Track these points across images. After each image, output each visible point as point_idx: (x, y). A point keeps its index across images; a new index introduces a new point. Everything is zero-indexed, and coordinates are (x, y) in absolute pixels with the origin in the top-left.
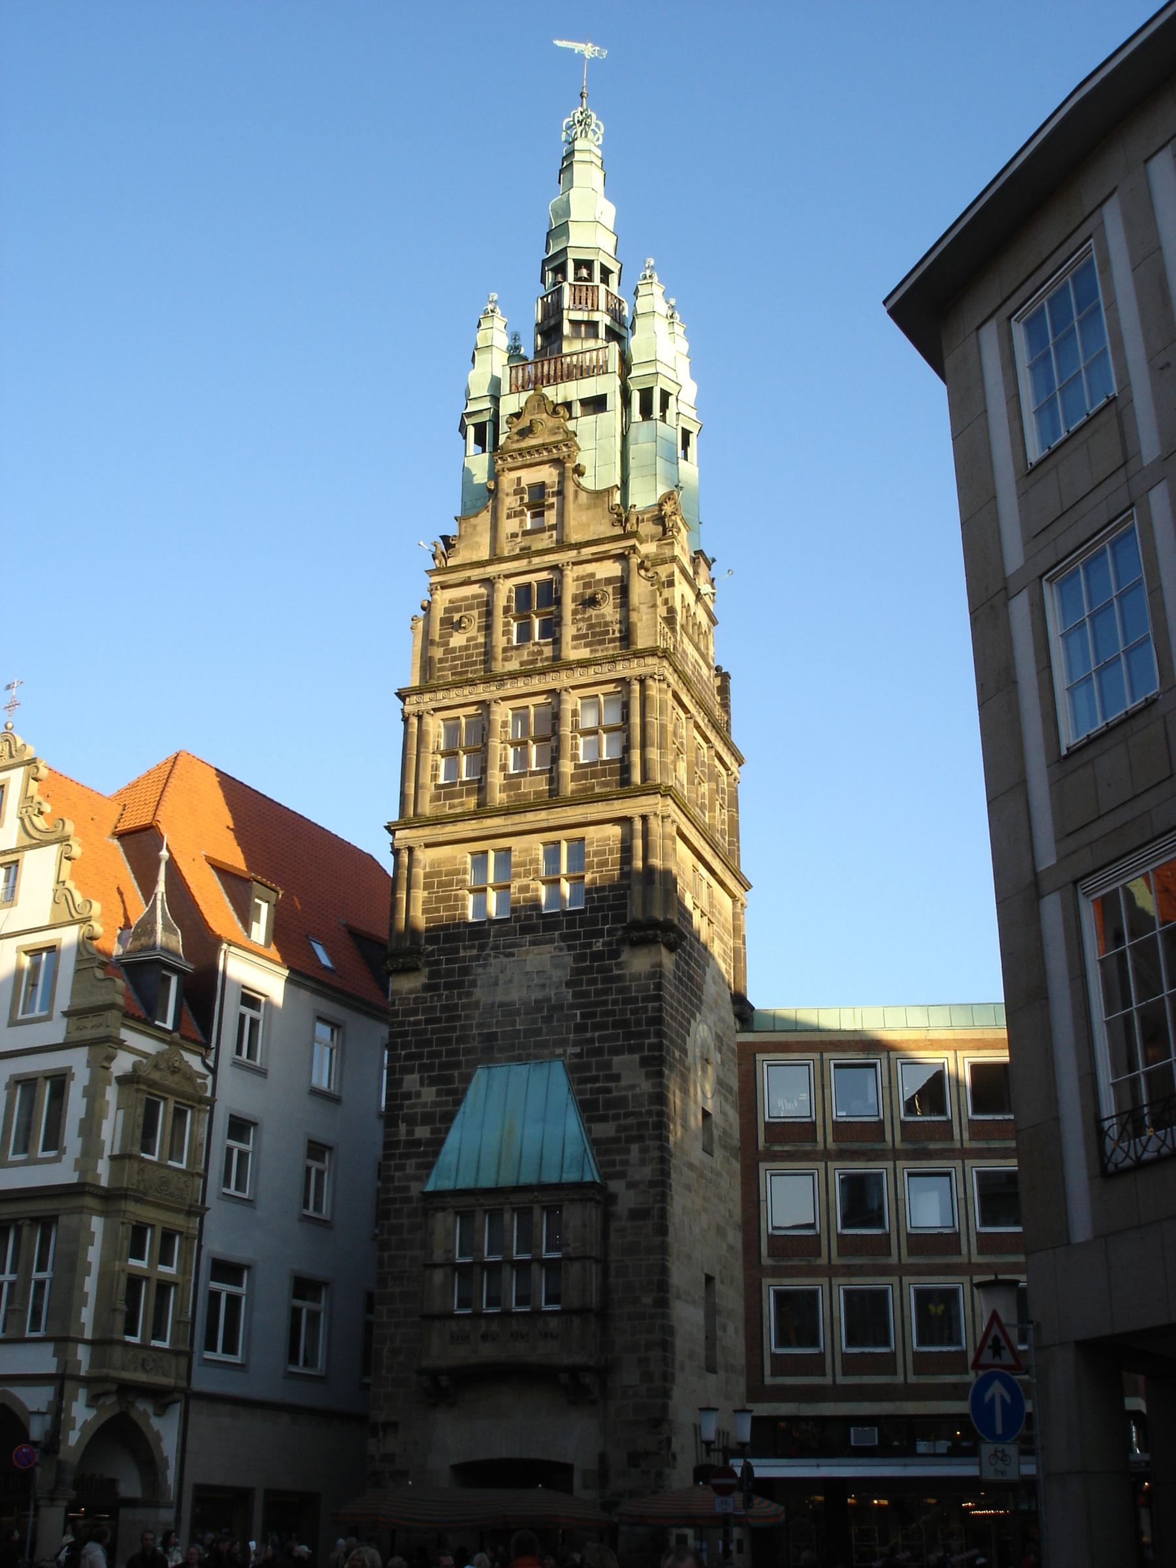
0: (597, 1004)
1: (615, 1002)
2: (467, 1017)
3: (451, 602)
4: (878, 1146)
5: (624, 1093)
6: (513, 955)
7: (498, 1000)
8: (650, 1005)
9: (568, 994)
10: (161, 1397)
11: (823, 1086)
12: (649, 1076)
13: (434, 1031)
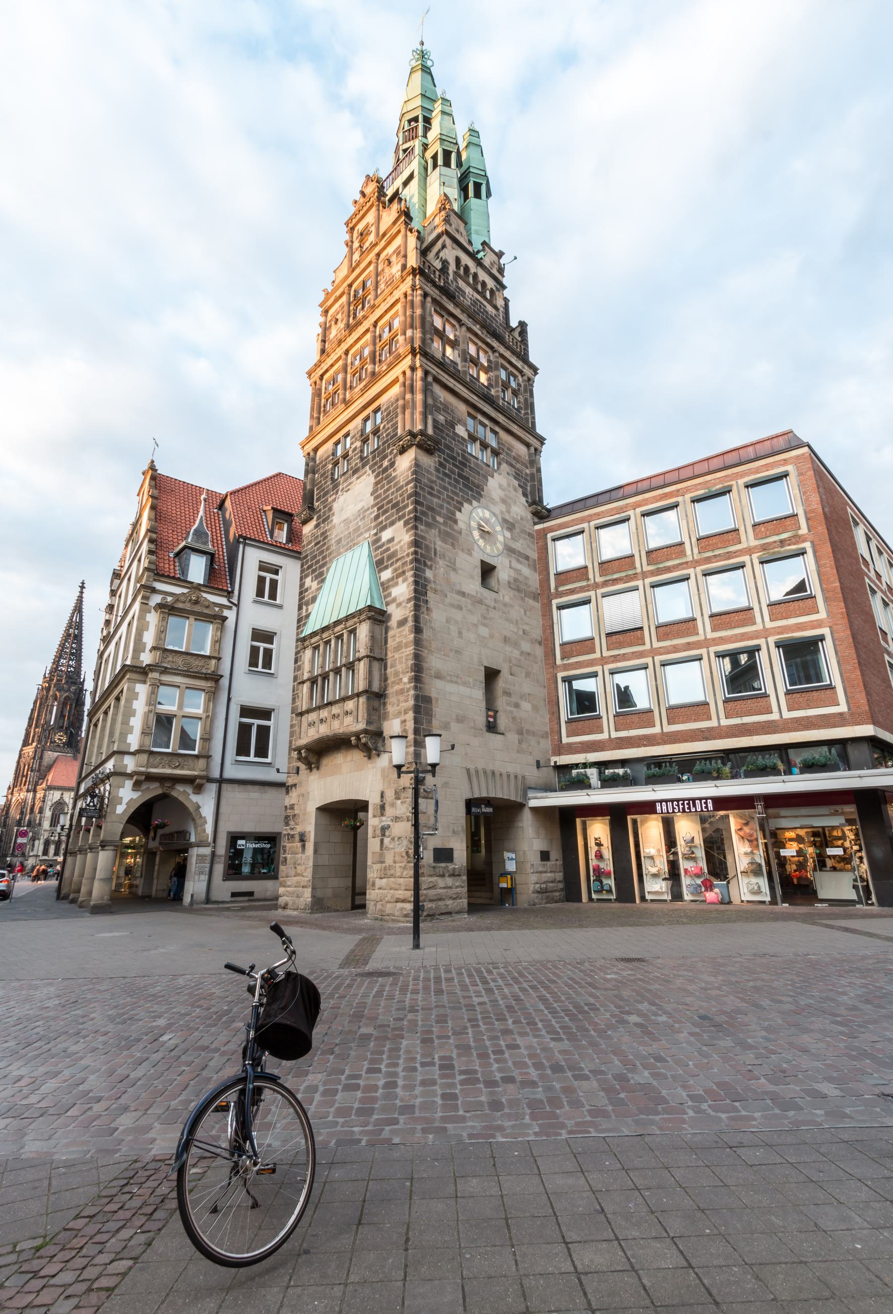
1: (393, 493)
4: (630, 572)
7: (343, 518)
8: (409, 486)
9: (371, 500)
10: (197, 784)
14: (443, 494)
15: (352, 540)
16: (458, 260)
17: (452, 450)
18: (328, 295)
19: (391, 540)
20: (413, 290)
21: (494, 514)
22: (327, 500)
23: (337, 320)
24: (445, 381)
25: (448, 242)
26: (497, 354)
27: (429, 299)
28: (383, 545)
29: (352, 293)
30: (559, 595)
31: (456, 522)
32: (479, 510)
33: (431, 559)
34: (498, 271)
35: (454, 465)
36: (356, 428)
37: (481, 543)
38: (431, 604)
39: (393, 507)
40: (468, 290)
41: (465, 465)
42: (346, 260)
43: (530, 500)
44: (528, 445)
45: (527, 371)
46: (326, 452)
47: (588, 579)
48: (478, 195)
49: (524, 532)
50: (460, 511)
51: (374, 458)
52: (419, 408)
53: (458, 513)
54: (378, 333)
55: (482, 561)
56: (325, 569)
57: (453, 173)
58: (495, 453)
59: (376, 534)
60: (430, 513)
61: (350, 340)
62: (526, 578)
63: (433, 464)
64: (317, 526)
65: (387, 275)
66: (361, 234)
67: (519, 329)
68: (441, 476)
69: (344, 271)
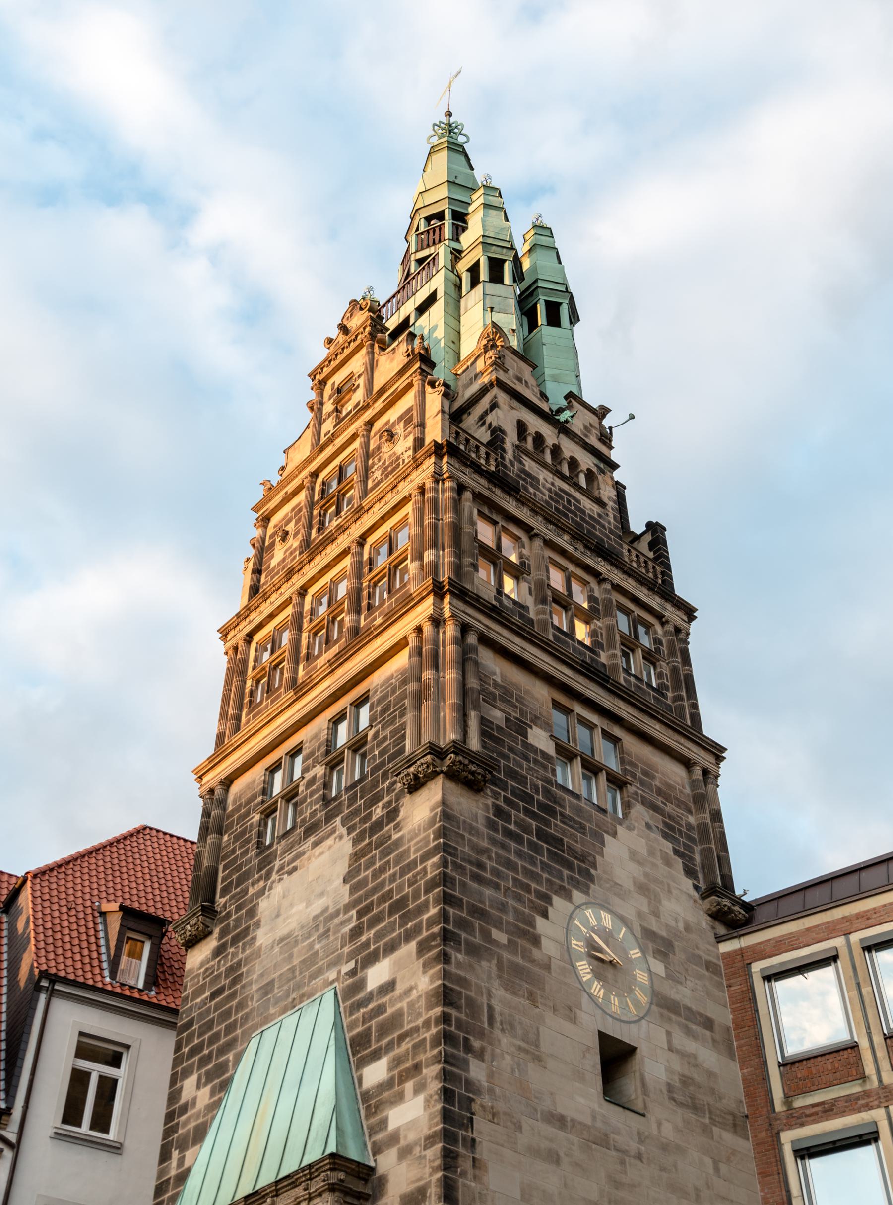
0: (374, 890)
1: (393, 878)
2: (248, 972)
3: (275, 527)
5: (399, 1006)
6: (295, 869)
9: (344, 894)
11: (858, 984)
12: (426, 966)
13: (217, 1008)
14: (506, 878)
15: (298, 987)
16: (521, 427)
17: (522, 780)
18: (271, 490)
19: (388, 987)
20: (437, 481)
21: (623, 920)
22: (246, 891)
23: (287, 533)
24: (504, 642)
25: (503, 398)
26: (608, 586)
27: (468, 495)
28: (370, 998)
29: (318, 487)
30: (799, 1118)
31: (536, 941)
32: (589, 912)
33: (481, 1035)
34: (600, 440)
35: (527, 812)
36: (316, 736)
37: (597, 989)
38: (484, 1151)
39: (393, 910)
40: (543, 475)
41: (552, 812)
42: (309, 432)
43: (702, 885)
44: (687, 763)
45: (674, 616)
46: (249, 787)
47: (863, 1078)
48: (554, 320)
49: (695, 959)
50: (545, 915)
51: (352, 800)
52: (451, 698)
53: (540, 921)
54: (366, 556)
55: (602, 1036)
56: (231, 1056)
57: (509, 290)
58: (617, 783)
59: (353, 973)
60: (477, 923)
61: (310, 571)
62: (711, 1075)
63: (481, 813)
64: (219, 951)
65: (386, 456)
66: (339, 391)
67: (648, 538)
68: (499, 837)
69: (304, 450)
